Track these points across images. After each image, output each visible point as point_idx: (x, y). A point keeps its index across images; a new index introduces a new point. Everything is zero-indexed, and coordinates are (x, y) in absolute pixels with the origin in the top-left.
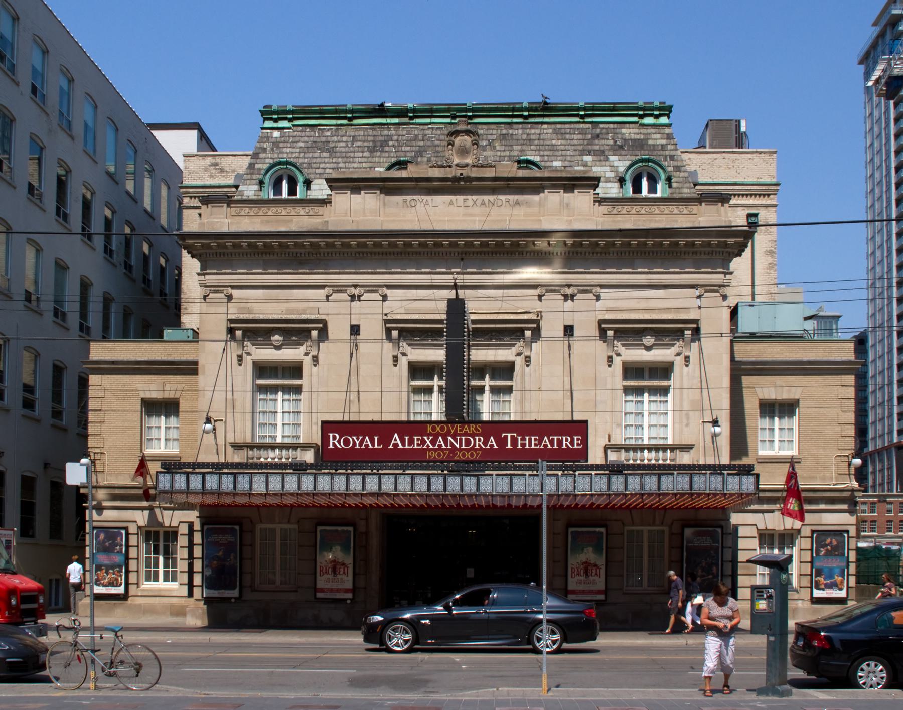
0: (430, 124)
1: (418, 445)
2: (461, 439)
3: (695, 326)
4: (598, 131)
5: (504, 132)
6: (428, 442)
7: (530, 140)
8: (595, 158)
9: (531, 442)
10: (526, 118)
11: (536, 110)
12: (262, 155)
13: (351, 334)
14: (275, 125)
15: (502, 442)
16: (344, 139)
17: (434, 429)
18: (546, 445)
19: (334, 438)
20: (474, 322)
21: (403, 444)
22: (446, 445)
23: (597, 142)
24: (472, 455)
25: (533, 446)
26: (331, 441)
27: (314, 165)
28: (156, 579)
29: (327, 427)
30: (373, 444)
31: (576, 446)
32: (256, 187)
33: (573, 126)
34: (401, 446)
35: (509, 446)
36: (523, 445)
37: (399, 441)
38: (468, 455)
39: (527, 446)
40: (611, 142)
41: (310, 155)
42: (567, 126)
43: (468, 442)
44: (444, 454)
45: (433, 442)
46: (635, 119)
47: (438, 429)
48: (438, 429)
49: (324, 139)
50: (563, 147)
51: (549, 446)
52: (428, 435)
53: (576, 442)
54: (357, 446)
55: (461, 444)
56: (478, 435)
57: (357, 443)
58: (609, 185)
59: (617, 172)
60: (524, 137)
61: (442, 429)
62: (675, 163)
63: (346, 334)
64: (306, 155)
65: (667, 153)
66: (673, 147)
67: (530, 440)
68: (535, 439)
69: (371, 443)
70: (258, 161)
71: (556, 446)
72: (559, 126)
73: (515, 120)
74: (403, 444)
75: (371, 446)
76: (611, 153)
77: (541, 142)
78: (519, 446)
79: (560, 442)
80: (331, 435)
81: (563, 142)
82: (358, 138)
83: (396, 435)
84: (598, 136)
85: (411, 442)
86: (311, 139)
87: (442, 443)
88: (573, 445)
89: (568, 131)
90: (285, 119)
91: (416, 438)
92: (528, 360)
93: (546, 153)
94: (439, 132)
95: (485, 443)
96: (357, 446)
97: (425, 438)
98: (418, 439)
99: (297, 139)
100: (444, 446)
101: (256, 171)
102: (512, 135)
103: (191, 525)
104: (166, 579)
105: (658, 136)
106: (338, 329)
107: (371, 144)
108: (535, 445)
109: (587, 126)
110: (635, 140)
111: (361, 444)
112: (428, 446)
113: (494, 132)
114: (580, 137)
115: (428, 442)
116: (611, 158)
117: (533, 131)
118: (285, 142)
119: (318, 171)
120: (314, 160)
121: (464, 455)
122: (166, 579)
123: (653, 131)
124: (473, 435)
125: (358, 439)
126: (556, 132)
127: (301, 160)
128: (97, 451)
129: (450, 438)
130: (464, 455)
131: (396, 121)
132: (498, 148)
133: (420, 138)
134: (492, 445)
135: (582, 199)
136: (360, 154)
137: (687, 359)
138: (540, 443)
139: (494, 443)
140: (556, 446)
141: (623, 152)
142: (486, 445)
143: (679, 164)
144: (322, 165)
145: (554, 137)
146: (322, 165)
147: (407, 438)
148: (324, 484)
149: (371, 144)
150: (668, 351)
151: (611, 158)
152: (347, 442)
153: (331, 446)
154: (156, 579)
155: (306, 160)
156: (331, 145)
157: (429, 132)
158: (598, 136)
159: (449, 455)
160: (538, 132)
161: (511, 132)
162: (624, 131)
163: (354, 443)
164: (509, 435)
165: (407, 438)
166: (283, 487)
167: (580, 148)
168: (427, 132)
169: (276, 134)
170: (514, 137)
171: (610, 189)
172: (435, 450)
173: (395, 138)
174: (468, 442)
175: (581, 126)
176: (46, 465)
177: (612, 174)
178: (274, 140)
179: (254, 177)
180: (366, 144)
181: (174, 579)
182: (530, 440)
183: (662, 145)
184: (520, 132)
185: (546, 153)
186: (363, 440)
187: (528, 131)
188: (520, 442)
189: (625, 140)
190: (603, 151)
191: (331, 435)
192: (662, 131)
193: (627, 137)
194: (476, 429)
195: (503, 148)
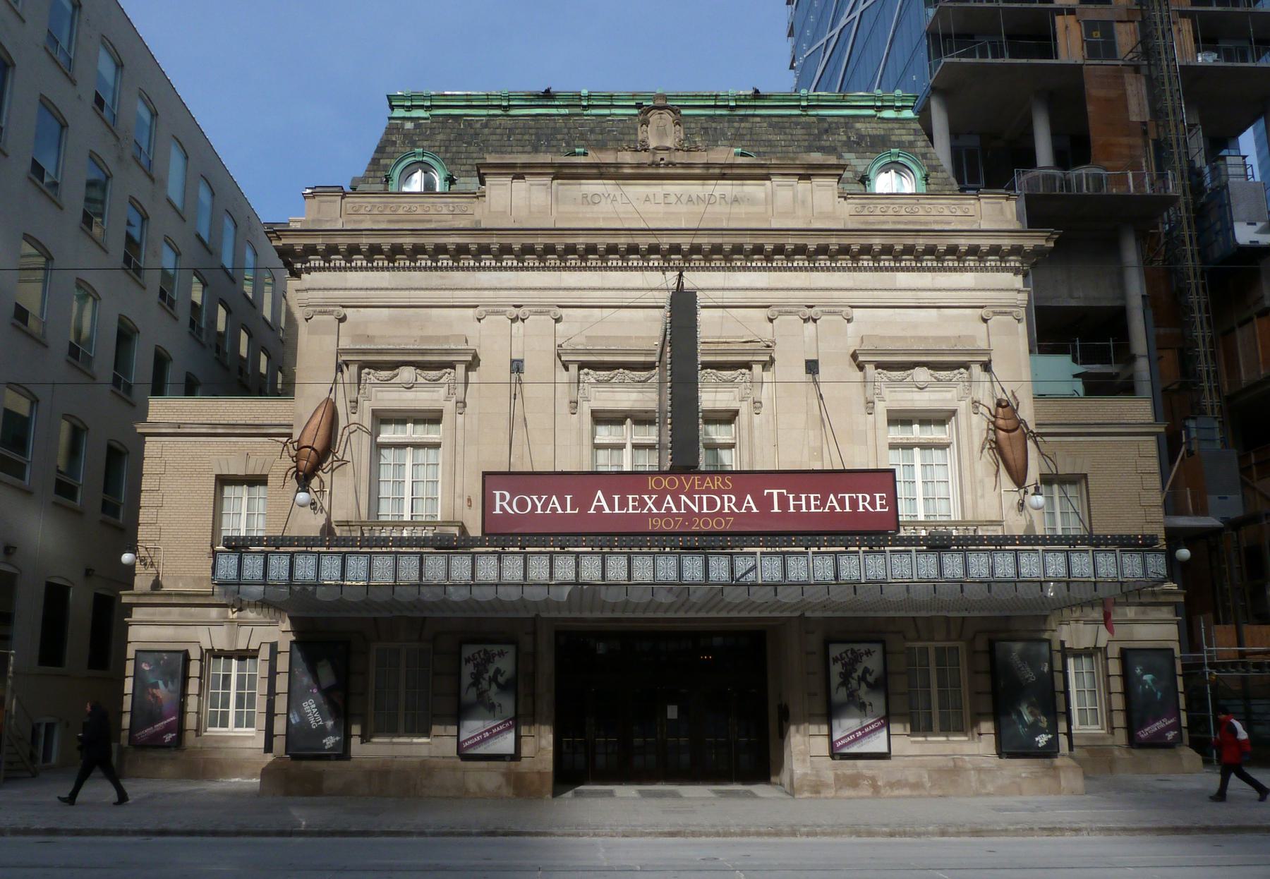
1: (634, 508)
2: (701, 500)
3: (985, 359)
4: (826, 125)
6: (650, 504)
9: (809, 503)
10: (732, 108)
11: (743, 100)
12: (389, 149)
14: (408, 114)
15: (764, 503)
16: (498, 131)
17: (658, 483)
18: (832, 508)
19: (503, 498)
21: (612, 508)
22: (678, 508)
24: (719, 523)
25: (813, 510)
28: (224, 724)
30: (564, 508)
31: (878, 509)
34: (607, 511)
35: (776, 510)
36: (798, 507)
37: (604, 503)
39: (804, 510)
40: (844, 138)
42: (785, 119)
43: (712, 504)
45: (658, 504)
46: (871, 112)
47: (665, 483)
48: (665, 483)
51: (838, 510)
52: (650, 493)
53: (878, 502)
54: (539, 511)
55: (701, 507)
57: (539, 505)
61: (672, 483)
62: (930, 162)
63: (505, 374)
67: (808, 499)
68: (816, 499)
69: (560, 506)
71: (848, 509)
72: (774, 119)
73: (718, 112)
74: (612, 508)
75: (560, 511)
76: (845, 149)
78: (792, 510)
79: (854, 503)
80: (498, 493)
83: (599, 493)
85: (623, 504)
87: (672, 505)
90: (421, 107)
91: (630, 497)
92: (757, 404)
96: (539, 511)
97: (646, 497)
98: (634, 500)
100: (675, 511)
103: (274, 646)
104: (238, 724)
105: (903, 132)
108: (816, 507)
111: (544, 507)
112: (650, 509)
115: (650, 504)
116: (847, 156)
121: (706, 523)
122: (238, 724)
123: (896, 126)
124: (720, 493)
126: (770, 125)
128: (149, 545)
129: (683, 497)
130: (706, 523)
131: (566, 111)
134: (749, 508)
138: (823, 504)
139: (752, 504)
140: (848, 509)
142: (739, 508)
143: (934, 163)
147: (616, 497)
148: (487, 569)
152: (522, 504)
153: (498, 511)
154: (224, 724)
158: (826, 131)
159: (683, 524)
160: (748, 125)
161: (714, 125)
162: (858, 125)
163: (534, 507)
164: (775, 492)
165: (616, 497)
167: (806, 144)
169: (409, 125)
172: (661, 516)
174: (712, 504)
175: (803, 119)
176: (88, 573)
179: (379, 174)
180: (526, 137)
181: (250, 724)
182: (808, 499)
187: (736, 125)
188: (792, 503)
191: (498, 493)
192: (907, 126)
193: (863, 131)
194: (724, 483)
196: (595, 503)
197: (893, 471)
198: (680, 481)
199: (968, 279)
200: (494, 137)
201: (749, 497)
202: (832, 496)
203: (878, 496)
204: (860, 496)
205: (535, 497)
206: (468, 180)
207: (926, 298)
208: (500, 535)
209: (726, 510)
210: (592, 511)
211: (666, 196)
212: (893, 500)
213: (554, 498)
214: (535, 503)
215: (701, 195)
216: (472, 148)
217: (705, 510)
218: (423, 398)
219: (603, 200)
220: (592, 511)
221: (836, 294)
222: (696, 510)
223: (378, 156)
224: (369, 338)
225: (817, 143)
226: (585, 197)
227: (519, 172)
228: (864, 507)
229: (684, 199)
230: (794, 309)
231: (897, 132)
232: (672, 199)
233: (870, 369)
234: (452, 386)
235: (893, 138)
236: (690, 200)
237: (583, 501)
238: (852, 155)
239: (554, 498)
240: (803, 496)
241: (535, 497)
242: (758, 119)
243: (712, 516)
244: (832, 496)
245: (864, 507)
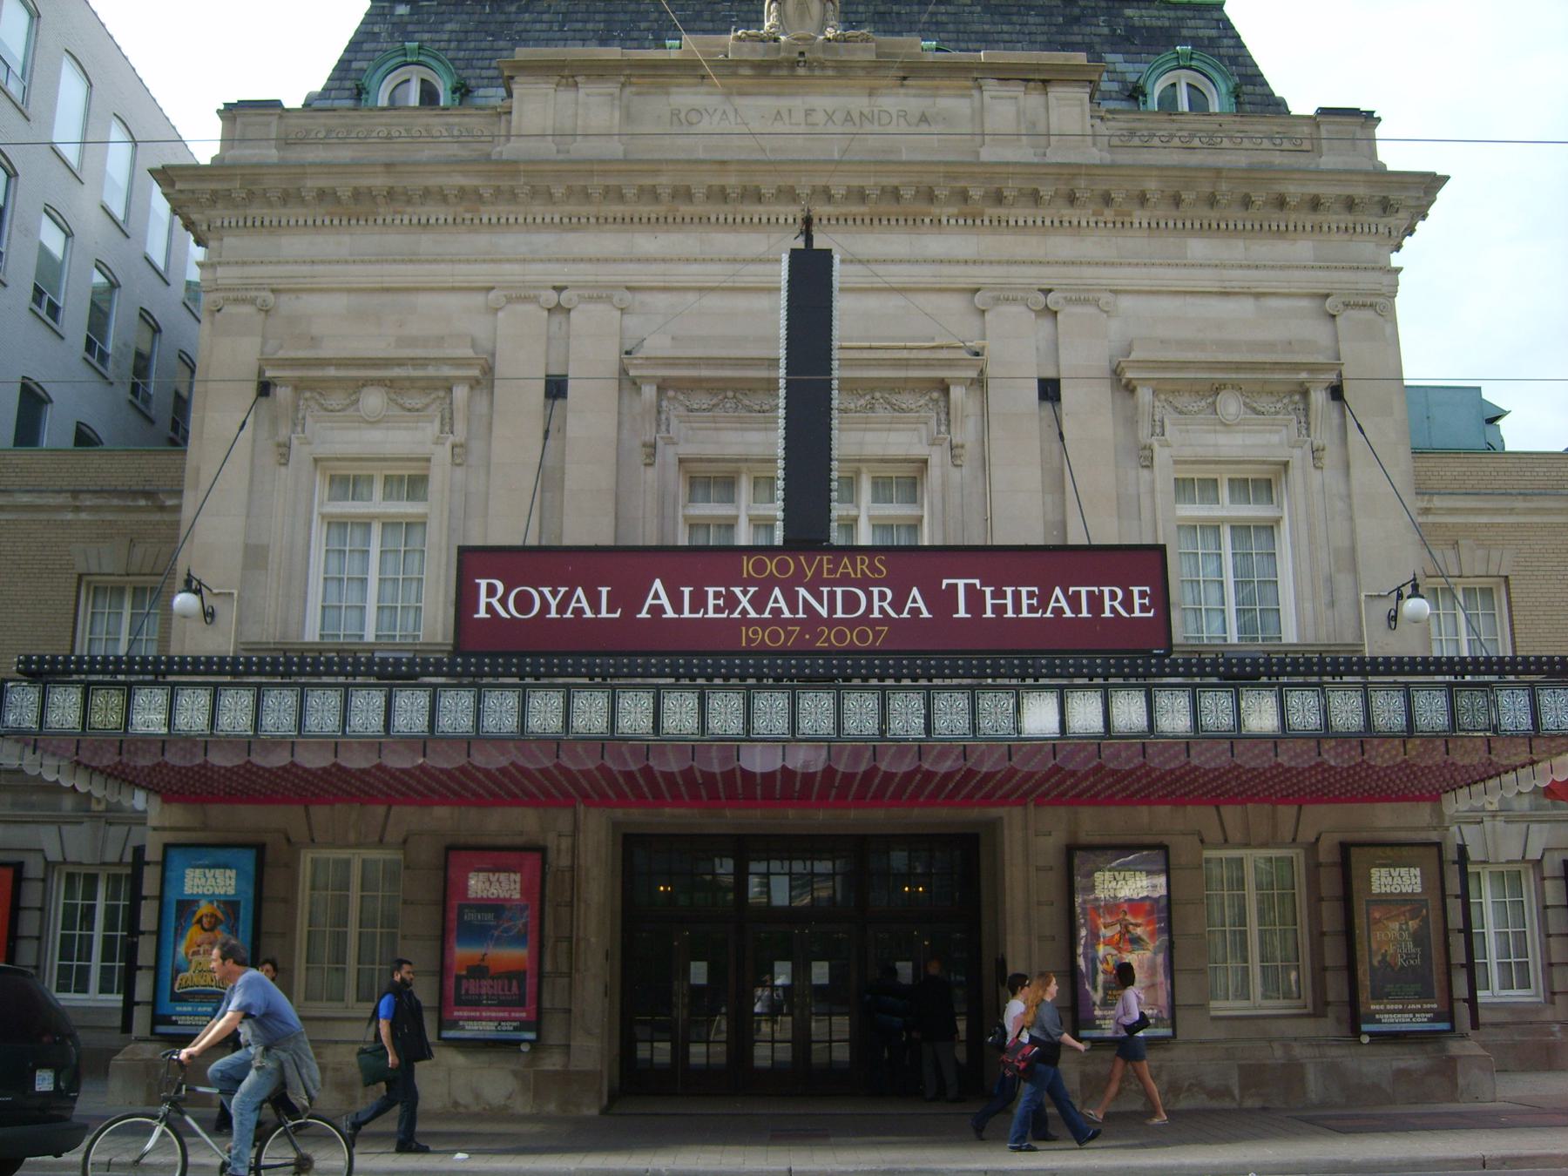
1: (717, 609)
2: (832, 595)
4: (1077, 11)
5: (882, 8)
6: (744, 602)
7: (937, 23)
9: (1018, 602)
15: (942, 601)
16: (546, 17)
17: (759, 567)
19: (491, 591)
21: (678, 608)
22: (793, 610)
23: (1076, 29)
24: (863, 636)
25: (1025, 614)
26: (483, 600)
27: (480, 64)
29: (474, 561)
30: (596, 607)
31: (1137, 613)
35: (962, 613)
38: (852, 637)
39: (1010, 614)
40: (1106, 31)
41: (472, 45)
43: (851, 603)
44: (789, 634)
45: (759, 602)
47: (771, 566)
48: (771, 566)
49: (503, 18)
51: (1068, 614)
52: (745, 584)
53: (1137, 601)
54: (553, 614)
55: (832, 609)
56: (877, 583)
57: (553, 603)
59: (1123, 82)
60: (925, 18)
61: (782, 567)
62: (1242, 70)
64: (465, 45)
65: (1222, 51)
66: (1232, 42)
67: (1017, 597)
68: (1030, 595)
69: (591, 605)
70: (359, 56)
71: (1085, 614)
74: (678, 608)
75: (589, 614)
76: (1106, 48)
77: (962, 27)
78: (989, 614)
79: (1096, 602)
80: (483, 583)
81: (1005, 28)
85: (699, 602)
86: (476, 17)
87: (782, 604)
88: (1130, 609)
91: (711, 590)
95: (898, 605)
96: (553, 614)
97: (737, 590)
98: (717, 595)
99: (446, 17)
100: (787, 614)
102: (898, 14)
105: (1200, 23)
108: (1031, 609)
110: (1148, 29)
111: (562, 608)
112: (744, 612)
115: (744, 602)
116: (1109, 57)
118: (419, 23)
119: (485, 73)
120: (480, 54)
121: (841, 636)
123: (1189, 14)
124: (865, 584)
125: (554, 594)
127: (451, 54)
129: (802, 591)
130: (841, 636)
133: (707, 15)
134: (915, 611)
137: (1316, 452)
138: (1043, 603)
139: (921, 604)
140: (1085, 614)
142: (899, 612)
143: (1250, 71)
145: (987, 18)
147: (687, 591)
149: (602, 26)
150: (1275, 439)
152: (524, 603)
153: (482, 613)
155: (461, 54)
156: (520, 27)
158: (1076, 20)
159: (801, 634)
161: (895, 8)
163: (545, 606)
164: (961, 583)
165: (687, 591)
166: (345, 720)
167: (1044, 38)
170: (904, 18)
173: (654, 16)
174: (851, 603)
177: (1115, 86)
178: (395, 20)
179: (348, 84)
180: (590, 26)
182: (1017, 597)
183: (1210, 39)
186: (568, 597)
188: (989, 602)
189: (1133, 27)
191: (483, 583)
192: (1207, 15)
193: (1137, 22)
196: (649, 601)
197: (1160, 550)
198: (798, 565)
199: (1302, 249)
200: (538, 26)
201: (915, 591)
202: (1057, 591)
203: (1136, 590)
204: (1106, 590)
205: (546, 590)
206: (491, 92)
207: (1237, 278)
208: (480, 653)
209: (876, 614)
210: (644, 614)
211: (809, 112)
212: (1161, 599)
213: (580, 592)
214: (547, 599)
215: (866, 111)
216: (501, 44)
217: (839, 614)
219: (706, 117)
220: (644, 614)
221: (1088, 272)
222: (824, 612)
223: (351, 56)
224: (314, 341)
225: (1063, 38)
226: (675, 113)
227: (567, 74)
228: (1113, 609)
229: (839, 117)
230: (1020, 295)
231: (1191, 23)
232: (819, 117)
233: (1144, 395)
234: (448, 423)
235: (1185, 32)
236: (849, 118)
237: (628, 597)
238: (1119, 57)
239: (580, 592)
240: (1009, 590)
241: (546, 590)
243: (851, 624)
244: (1057, 591)
245: (1113, 609)
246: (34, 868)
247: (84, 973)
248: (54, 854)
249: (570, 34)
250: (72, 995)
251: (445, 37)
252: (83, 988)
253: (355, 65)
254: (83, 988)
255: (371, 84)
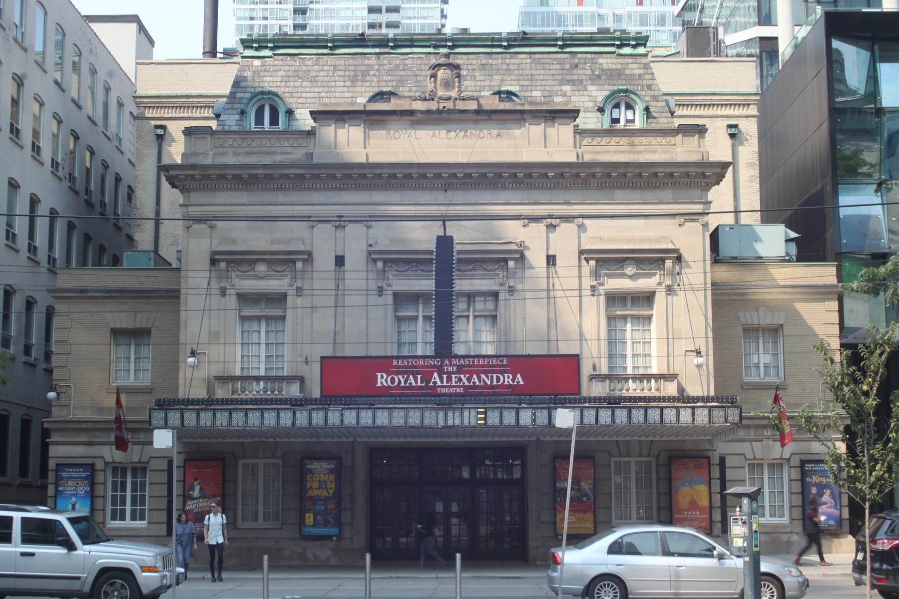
0: (410, 54)
2: (492, 377)
4: (576, 61)
5: (484, 62)
8: (574, 88)
13: (336, 265)
16: (326, 68)
20: (459, 252)
23: (575, 71)
27: (296, 95)
32: (237, 117)
33: (551, 56)
40: (589, 72)
49: (305, 68)
50: (541, 77)
58: (588, 115)
59: (596, 102)
60: (504, 67)
63: (331, 265)
64: (288, 84)
65: (644, 82)
70: (239, 90)
72: (537, 56)
73: (494, 50)
76: (589, 82)
77: (521, 72)
81: (542, 72)
82: (339, 68)
84: (576, 66)
86: (292, 68)
89: (547, 61)
93: (526, 83)
94: (419, 62)
101: (237, 101)
106: (324, 261)
107: (352, 73)
109: (566, 56)
110: (610, 70)
113: (474, 62)
114: (558, 67)
116: (590, 88)
117: (512, 61)
118: (266, 71)
120: (296, 90)
127: (282, 90)
132: (478, 78)
133: (401, 67)
134: (518, 382)
135: (563, 132)
136: (342, 84)
139: (520, 380)
141: (601, 82)
144: (304, 95)
146: (304, 95)
151: (590, 88)
157: (408, 62)
160: (517, 61)
161: (490, 61)
162: (601, 61)
167: (559, 77)
168: (407, 62)
170: (494, 67)
171: (589, 120)
173: (376, 67)
175: (559, 56)
178: (254, 69)
179: (235, 106)
180: (347, 73)
184: (500, 61)
185: (526, 83)
187: (508, 61)
189: (603, 70)
190: (581, 82)
193: (605, 67)
195: (483, 78)
218: (275, 285)
222: (489, 383)
223: (235, 90)
225: (568, 77)
231: (631, 66)
242: (525, 56)
246: (99, 465)
247: (123, 512)
248: (108, 459)
249: (337, 78)
250: (118, 522)
251: (279, 79)
252: (123, 518)
253: (238, 95)
254: (123, 518)
255: (248, 111)
